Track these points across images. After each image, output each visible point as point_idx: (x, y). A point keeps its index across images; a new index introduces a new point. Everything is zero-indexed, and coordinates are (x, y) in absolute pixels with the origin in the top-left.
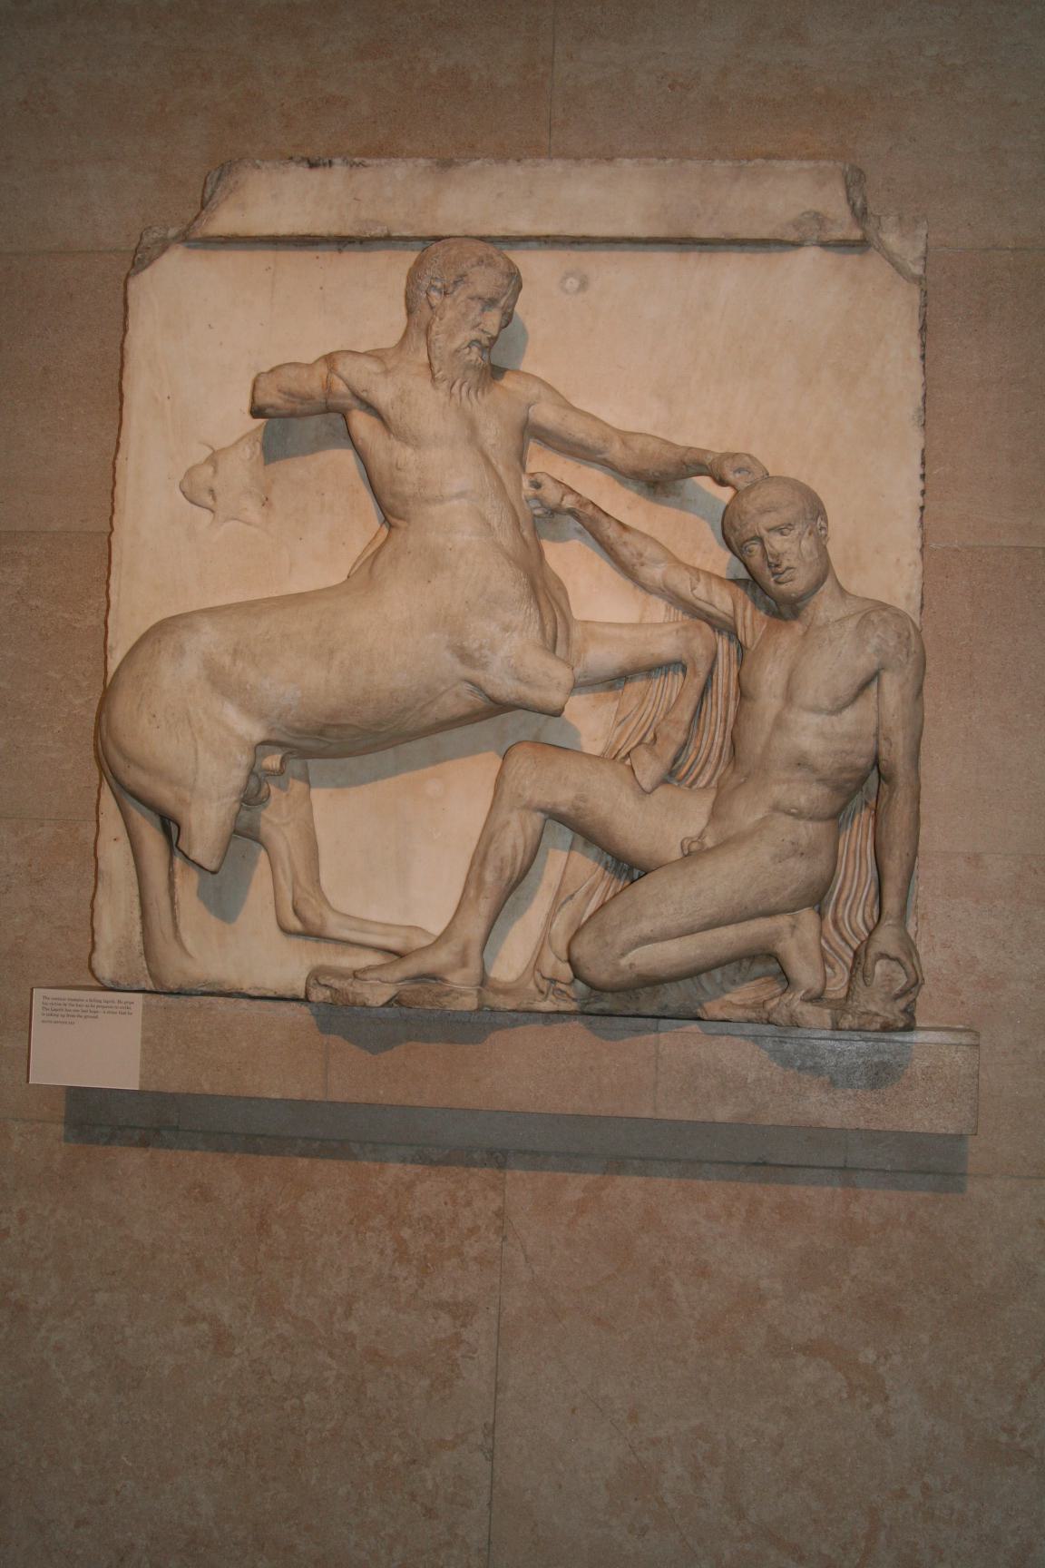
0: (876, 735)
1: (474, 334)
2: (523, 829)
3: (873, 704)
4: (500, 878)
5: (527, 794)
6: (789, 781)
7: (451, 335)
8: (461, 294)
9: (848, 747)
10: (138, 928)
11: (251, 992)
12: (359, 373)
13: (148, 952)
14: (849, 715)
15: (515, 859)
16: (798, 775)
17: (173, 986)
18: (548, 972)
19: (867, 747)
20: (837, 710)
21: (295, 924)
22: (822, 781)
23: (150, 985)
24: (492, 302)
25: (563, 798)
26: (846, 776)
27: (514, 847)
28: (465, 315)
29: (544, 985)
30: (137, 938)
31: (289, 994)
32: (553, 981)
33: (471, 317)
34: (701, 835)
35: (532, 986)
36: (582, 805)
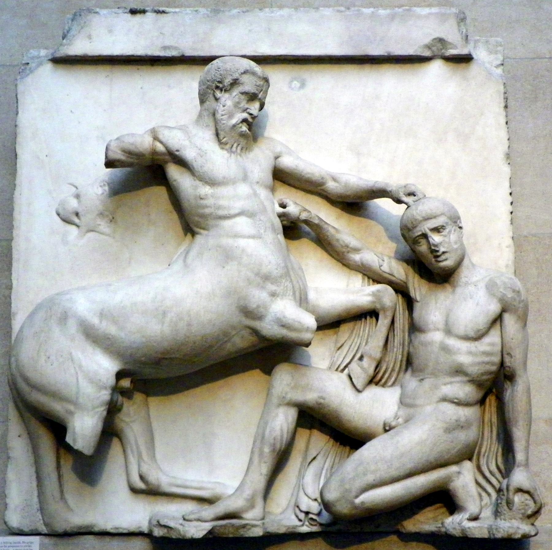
0: (502, 352)
1: (245, 115)
2: (286, 419)
3: (499, 333)
4: (274, 450)
5: (289, 396)
6: (451, 383)
7: (231, 116)
8: (236, 92)
9: (487, 359)
10: (36, 493)
11: (112, 531)
12: (175, 140)
13: (42, 509)
14: (487, 340)
15: (282, 436)
16: (458, 379)
17: (60, 530)
18: (304, 508)
19: (497, 359)
20: (478, 337)
21: (141, 485)
22: (472, 381)
23: (44, 530)
24: (252, 97)
25: (310, 397)
26: (485, 377)
27: (282, 430)
28: (239, 103)
29: (302, 516)
30: (36, 500)
31: (137, 531)
32: (307, 513)
33: (242, 105)
34: (396, 417)
35: (294, 517)
36: (322, 401)
